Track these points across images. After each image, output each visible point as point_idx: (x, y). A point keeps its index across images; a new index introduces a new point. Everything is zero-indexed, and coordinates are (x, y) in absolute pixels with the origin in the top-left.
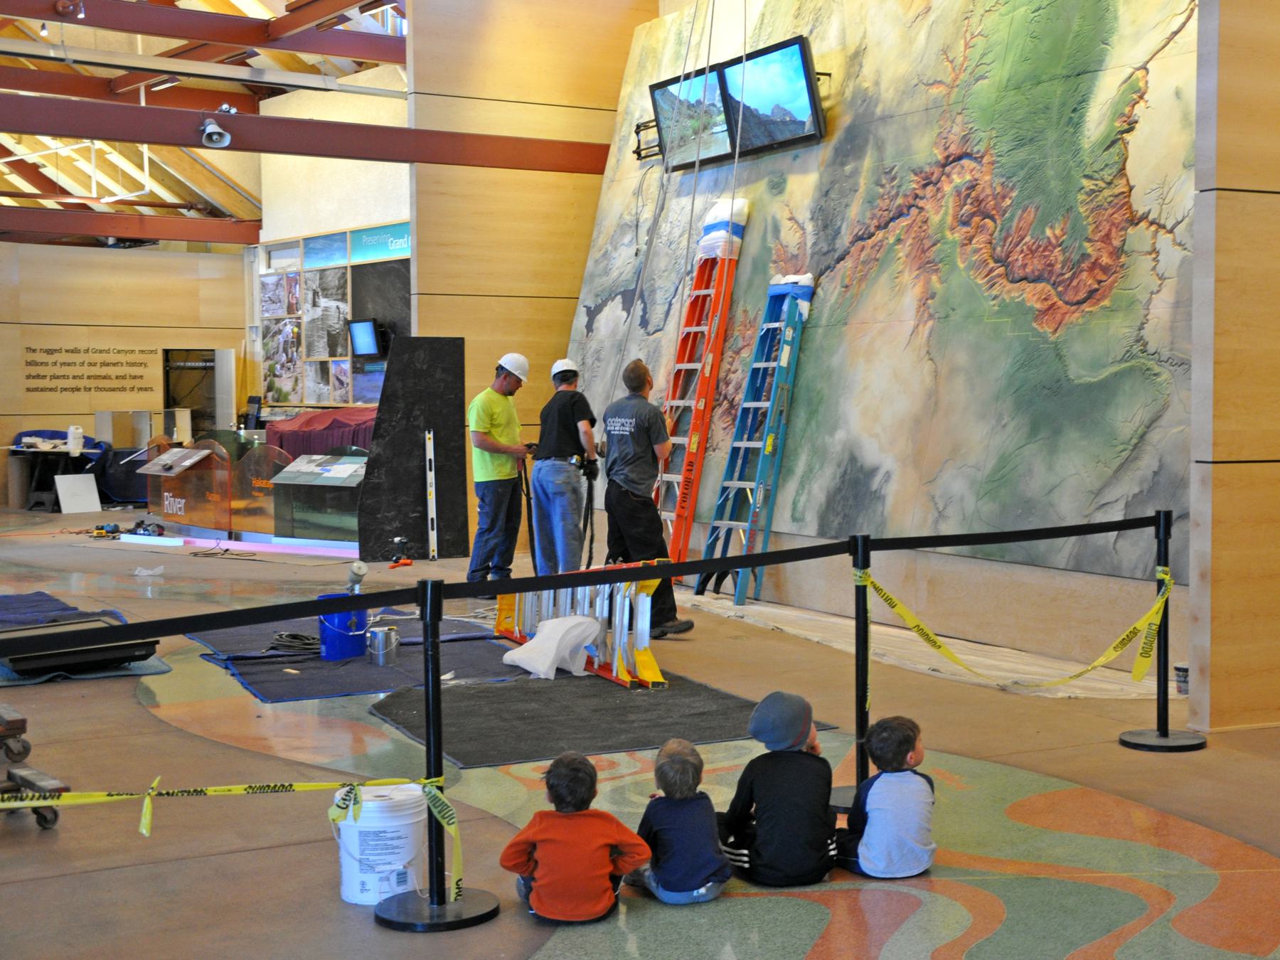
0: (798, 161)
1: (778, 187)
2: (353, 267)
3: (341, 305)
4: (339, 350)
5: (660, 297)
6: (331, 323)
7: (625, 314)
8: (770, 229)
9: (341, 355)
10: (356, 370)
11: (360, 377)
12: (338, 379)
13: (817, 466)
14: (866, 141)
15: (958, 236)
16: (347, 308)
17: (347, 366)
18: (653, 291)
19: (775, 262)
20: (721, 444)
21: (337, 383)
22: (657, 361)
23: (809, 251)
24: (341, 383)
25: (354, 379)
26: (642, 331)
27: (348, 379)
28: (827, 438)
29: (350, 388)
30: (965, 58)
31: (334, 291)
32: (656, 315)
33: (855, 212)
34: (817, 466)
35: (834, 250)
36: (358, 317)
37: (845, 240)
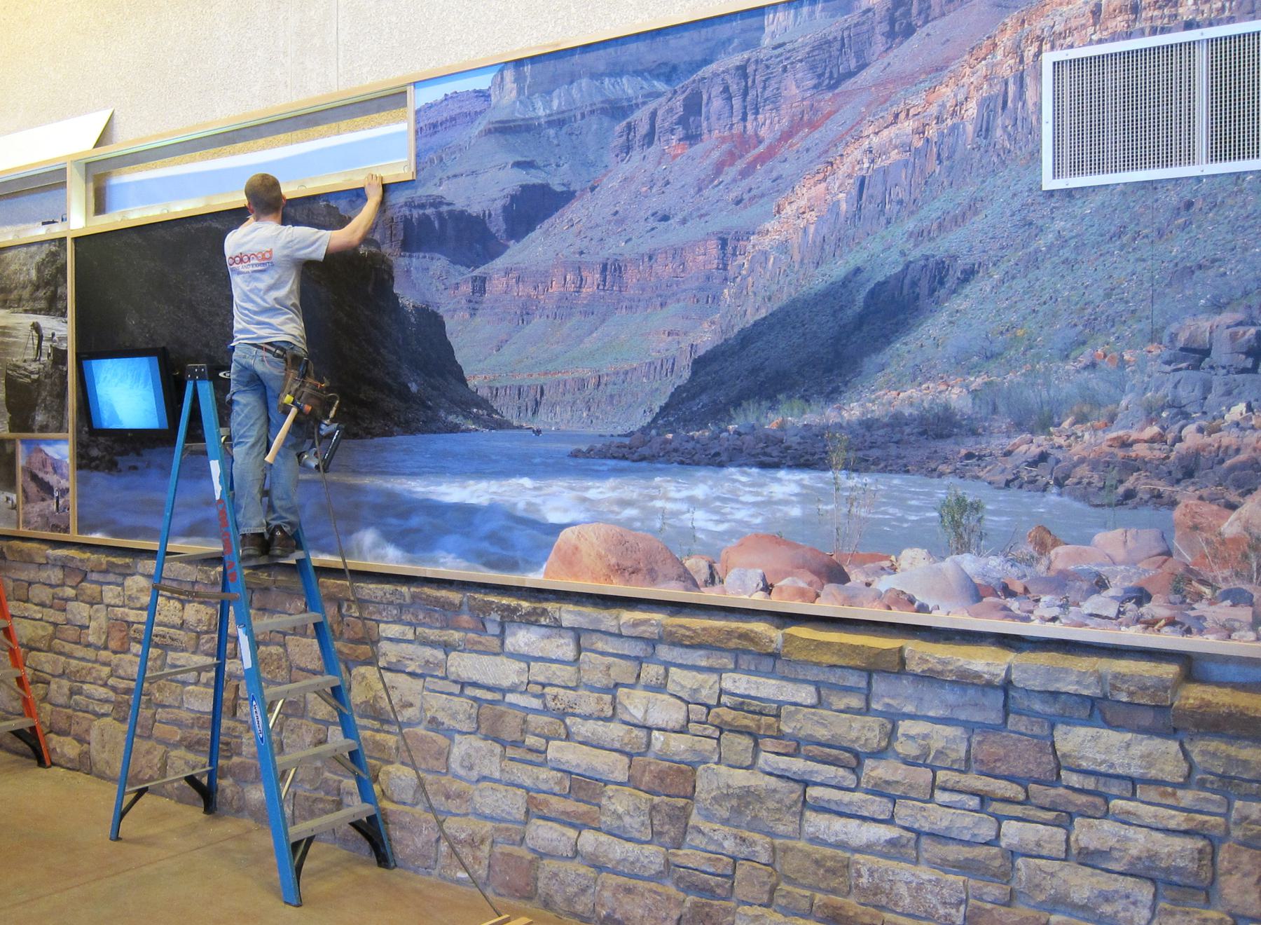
2: (76, 240)
3: (49, 324)
4: (40, 418)
6: (17, 359)
9: (43, 429)
10: (84, 461)
11: (99, 479)
12: (34, 477)
16: (62, 329)
17: (62, 450)
21: (33, 488)
24: (46, 488)
25: (81, 482)
27: (67, 479)
29: (72, 498)
31: (26, 294)
36: (99, 340)
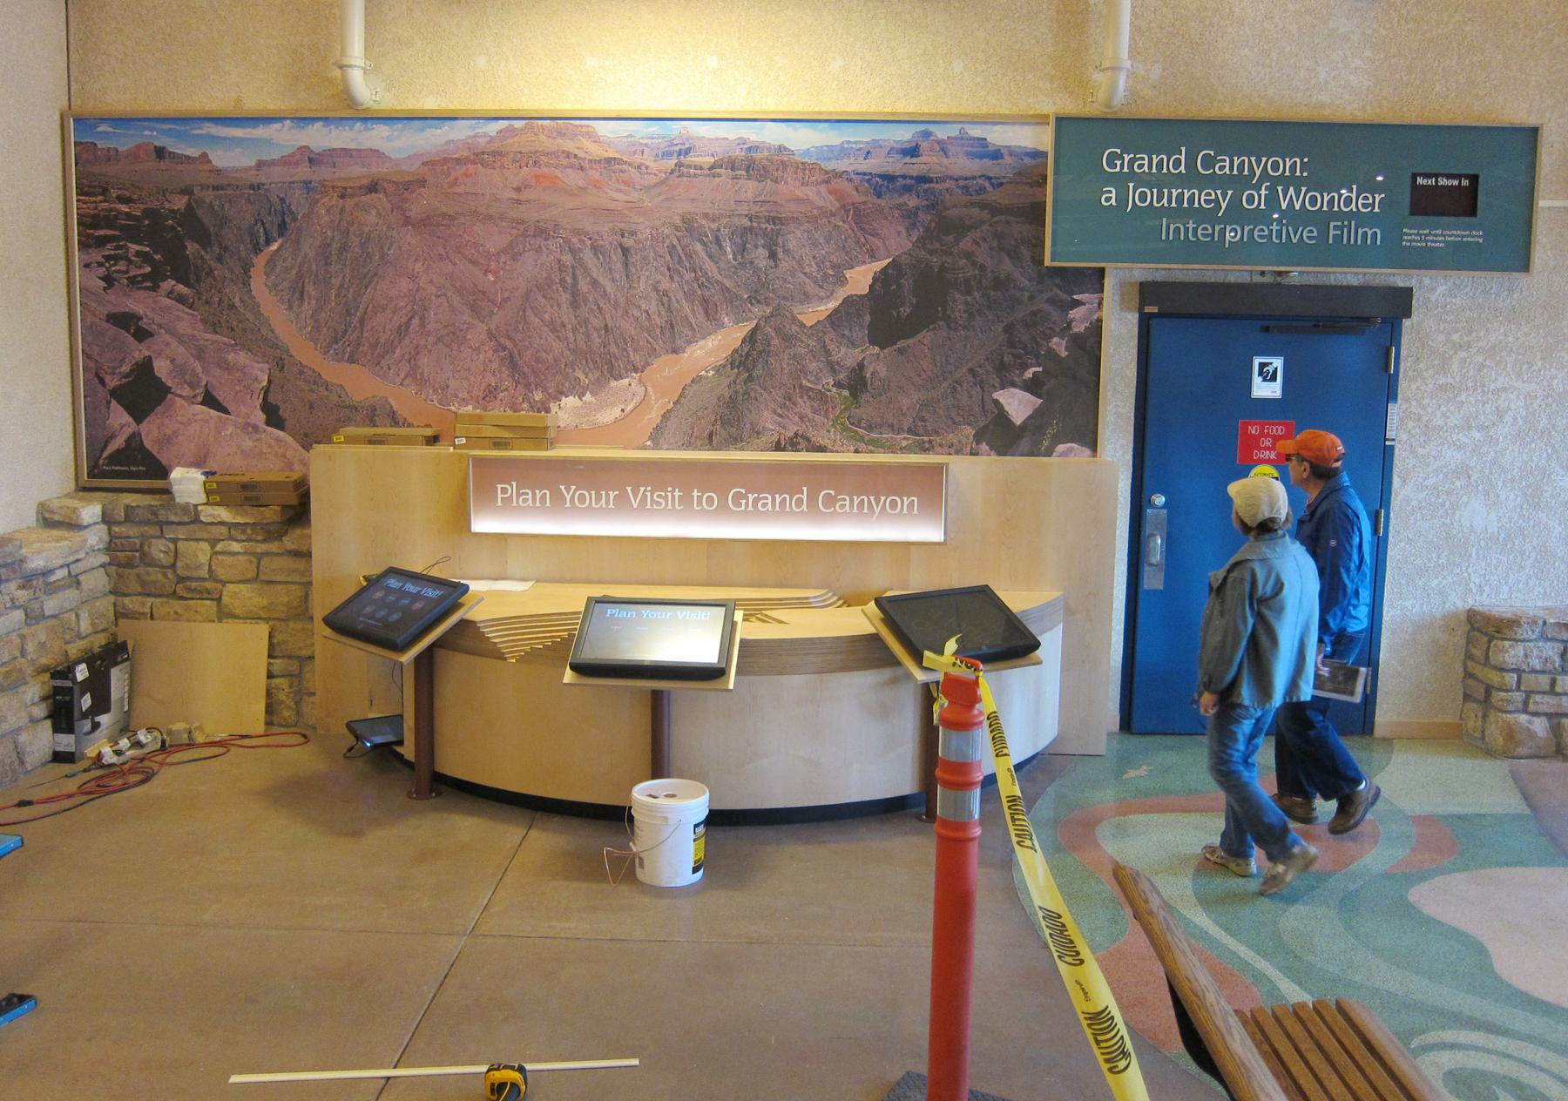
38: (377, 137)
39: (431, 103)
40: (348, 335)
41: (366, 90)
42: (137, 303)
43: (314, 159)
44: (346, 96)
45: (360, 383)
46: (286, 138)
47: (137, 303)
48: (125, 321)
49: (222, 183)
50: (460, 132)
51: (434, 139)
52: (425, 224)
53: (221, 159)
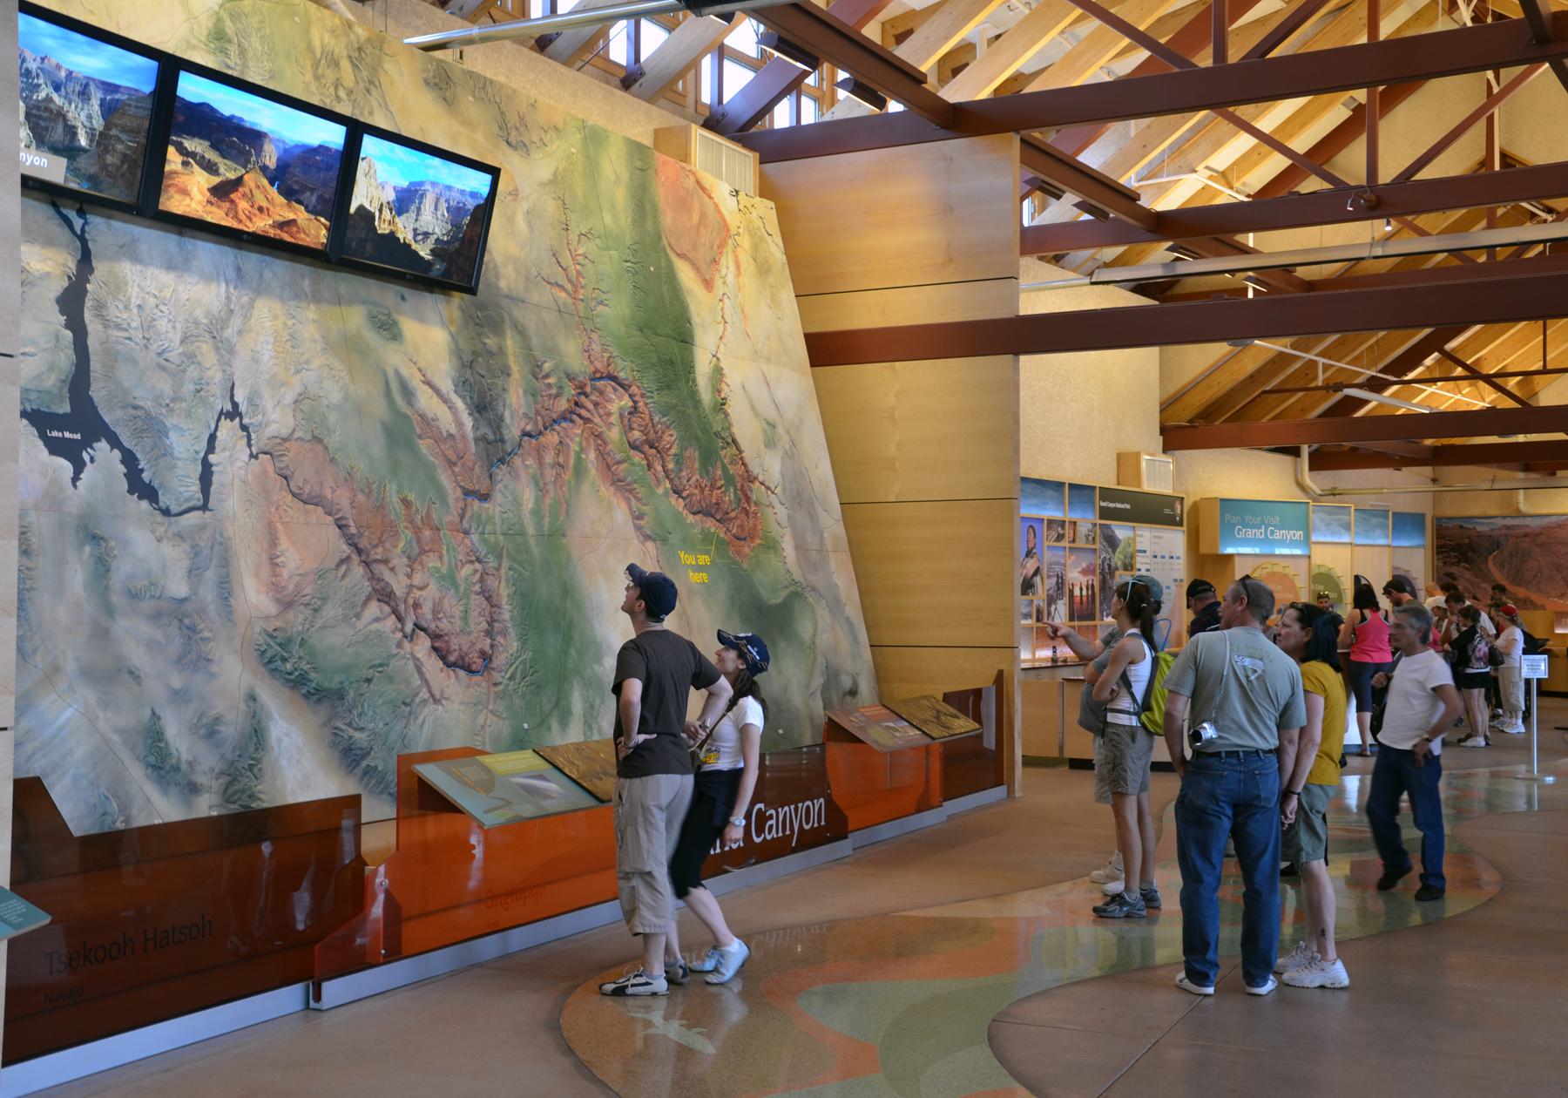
0: (406, 306)
1: (388, 328)
5: (184, 444)
7: (66, 466)
8: (394, 386)
13: (598, 702)
14: (503, 322)
15: (637, 458)
18: (153, 427)
19: (420, 437)
20: (448, 692)
22: (225, 563)
23: (470, 435)
26: (145, 504)
28: (596, 667)
30: (579, 274)
32: (182, 484)
33: (515, 403)
34: (598, 702)
35: (502, 441)
37: (513, 428)
38: (1528, 521)
39: (1544, 511)
40: (1518, 580)
41: (1523, 507)
42: (1454, 570)
43: (1507, 528)
44: (1519, 511)
45: (1521, 592)
46: (1500, 522)
47: (1454, 570)
48: (1449, 575)
49: (1480, 535)
50: (1553, 519)
51: (1546, 521)
52: (1542, 545)
53: (1479, 528)
